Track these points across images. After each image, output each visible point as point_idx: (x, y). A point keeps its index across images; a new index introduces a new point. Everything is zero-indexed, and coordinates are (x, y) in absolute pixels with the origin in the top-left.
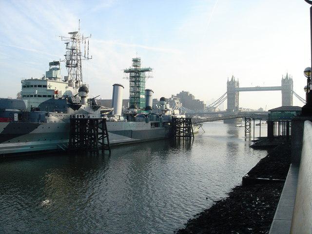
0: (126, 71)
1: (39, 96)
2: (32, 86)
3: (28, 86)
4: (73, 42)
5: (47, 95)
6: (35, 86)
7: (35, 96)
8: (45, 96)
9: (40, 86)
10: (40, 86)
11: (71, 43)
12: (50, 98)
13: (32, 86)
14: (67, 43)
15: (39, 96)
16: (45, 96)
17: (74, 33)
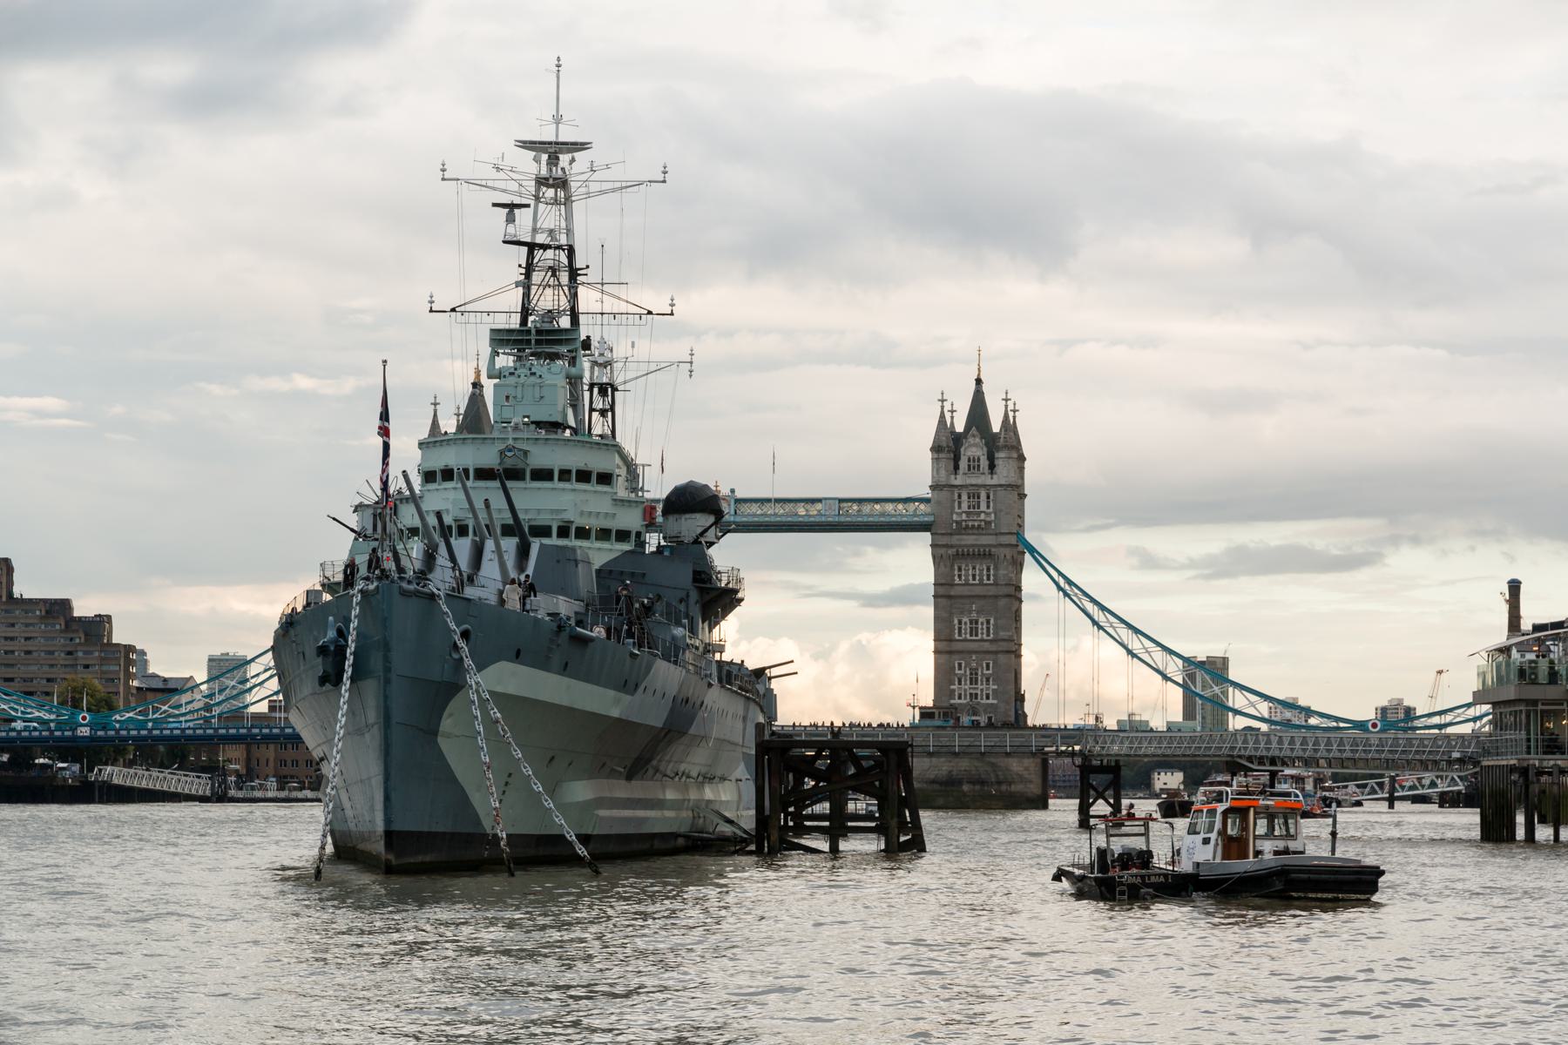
1: (583, 533)
2: (543, 475)
4: (537, 198)
5: (616, 524)
6: (565, 475)
7: (563, 532)
8: (604, 534)
9: (584, 476)
10: (584, 476)
11: (532, 203)
12: (626, 547)
13: (543, 475)
14: (512, 207)
15: (583, 533)
16: (604, 534)
17: (553, 150)
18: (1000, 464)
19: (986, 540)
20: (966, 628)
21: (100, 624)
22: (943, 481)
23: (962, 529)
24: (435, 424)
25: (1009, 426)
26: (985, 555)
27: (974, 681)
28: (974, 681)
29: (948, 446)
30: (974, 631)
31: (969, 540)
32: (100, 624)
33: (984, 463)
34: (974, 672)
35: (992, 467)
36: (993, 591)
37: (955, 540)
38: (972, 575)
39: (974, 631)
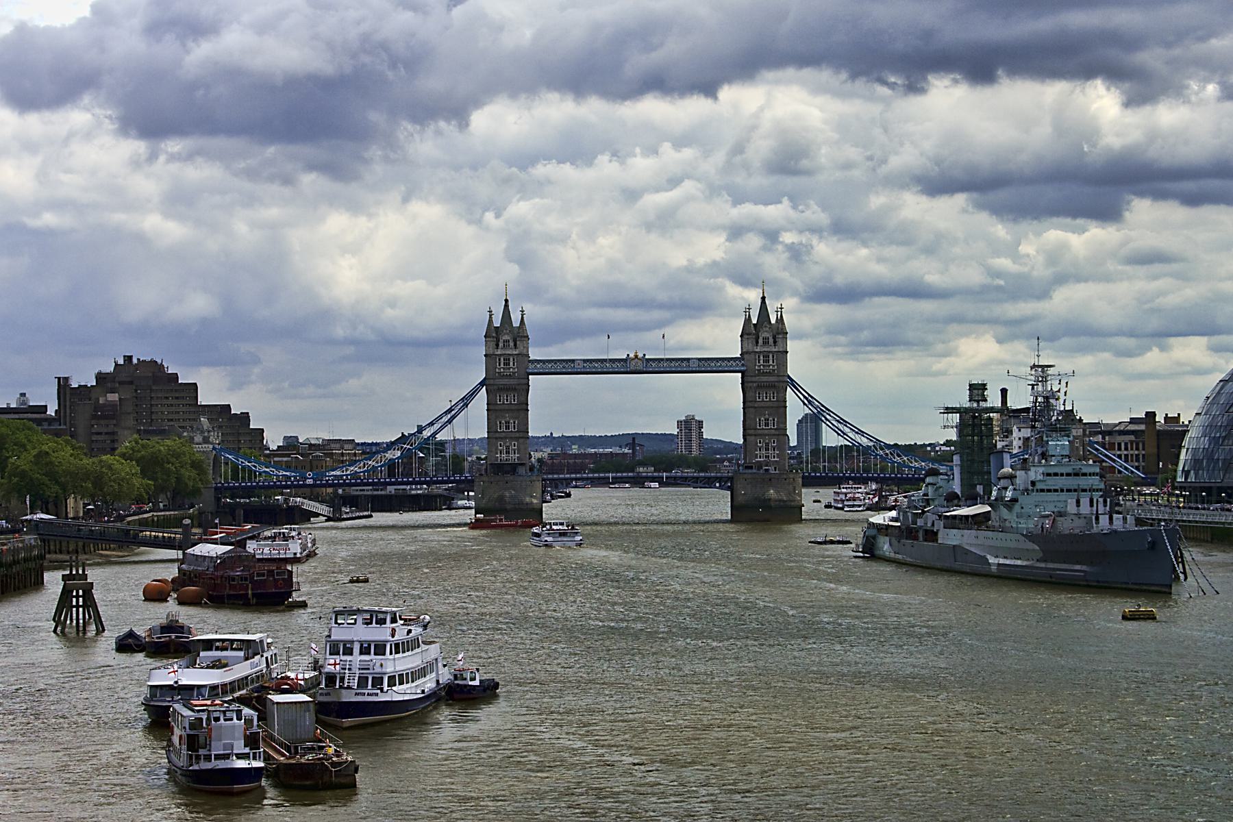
0: (949, 410)
2: (1084, 475)
3: (1076, 475)
13: (1084, 475)
17: (1043, 367)
18: (780, 341)
19: (772, 379)
20: (763, 423)
21: (245, 417)
22: (750, 347)
23: (760, 373)
24: (490, 321)
25: (780, 320)
26: (771, 386)
27: (767, 449)
28: (767, 449)
29: (750, 332)
30: (767, 425)
31: (765, 379)
32: (245, 417)
33: (771, 340)
34: (767, 444)
35: (775, 342)
36: (776, 404)
37: (754, 379)
38: (766, 397)
39: (767, 425)
